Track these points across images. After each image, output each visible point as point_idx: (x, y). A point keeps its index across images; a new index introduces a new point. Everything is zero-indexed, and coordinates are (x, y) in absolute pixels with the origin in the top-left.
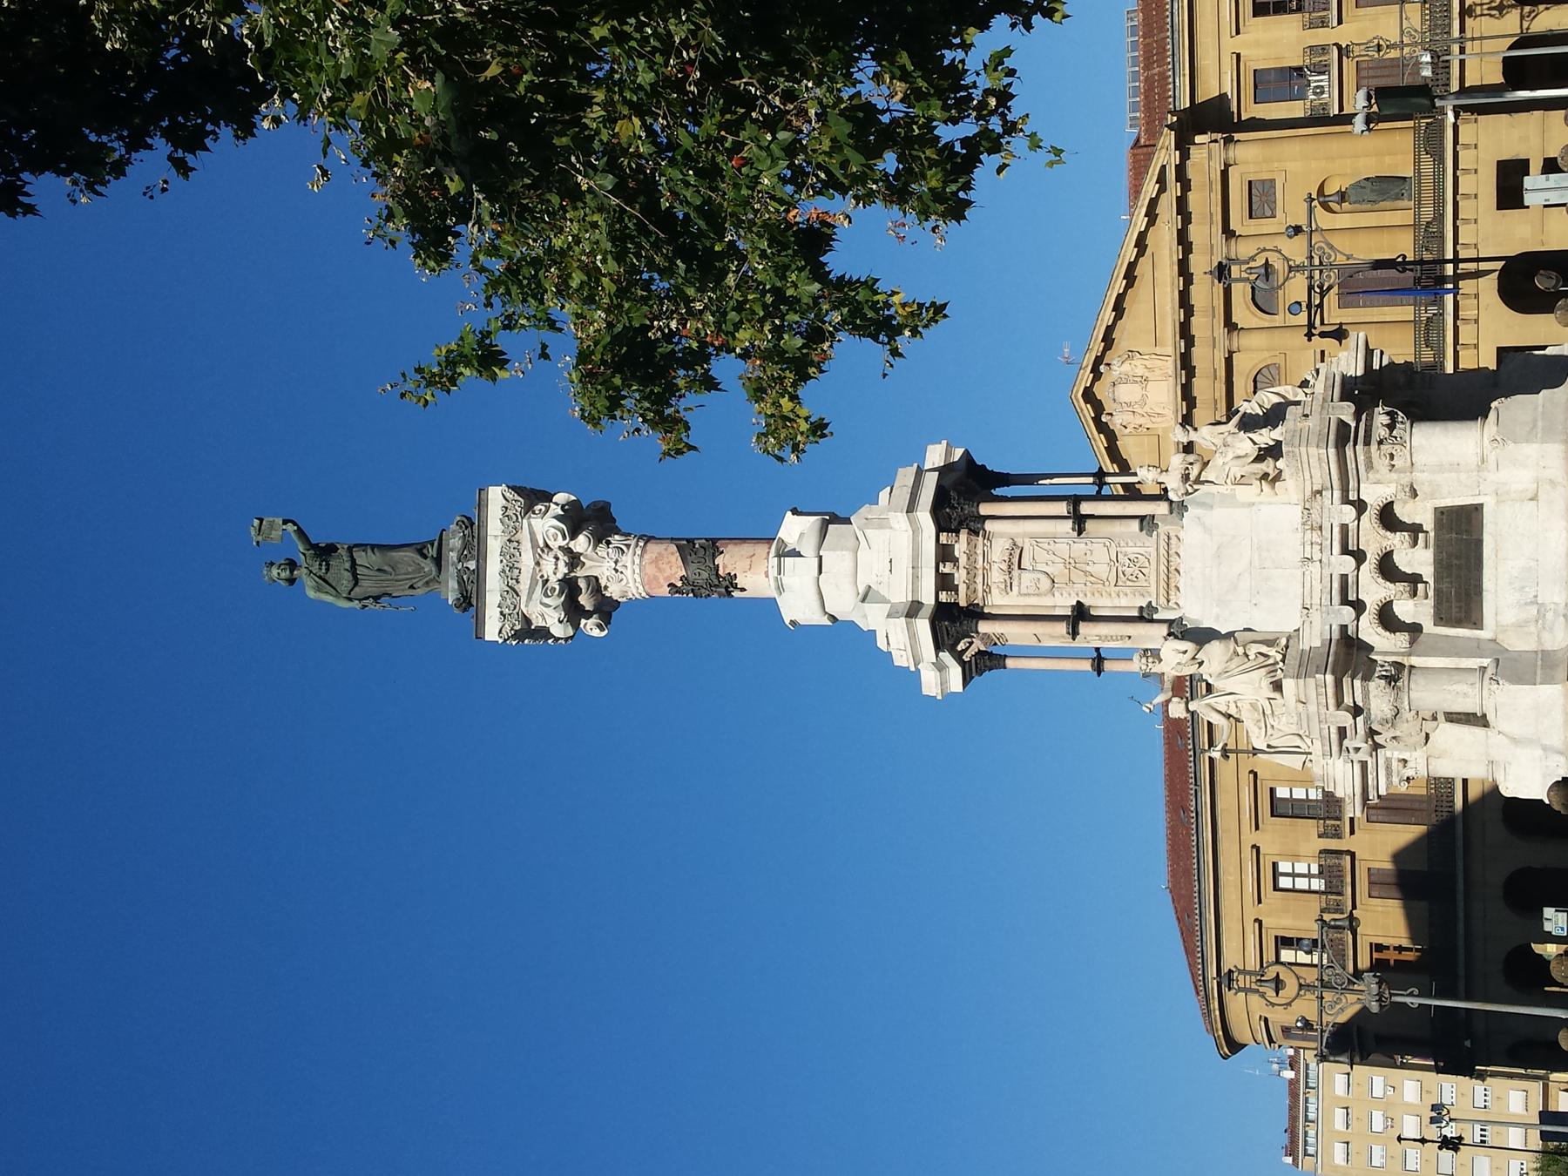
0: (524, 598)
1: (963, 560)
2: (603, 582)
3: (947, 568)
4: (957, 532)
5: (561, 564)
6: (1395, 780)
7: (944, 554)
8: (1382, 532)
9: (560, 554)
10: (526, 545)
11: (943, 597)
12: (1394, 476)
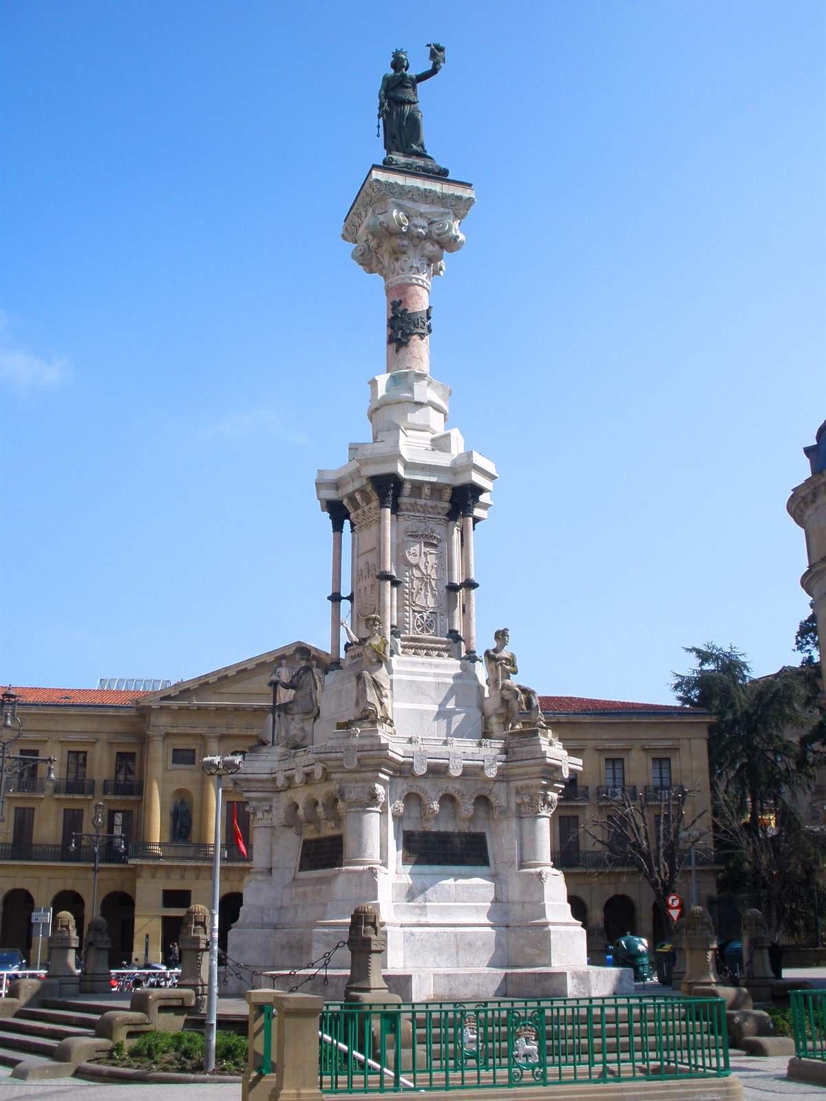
0: (397, 201)
1: (430, 503)
2: (404, 257)
3: (426, 491)
4: (450, 502)
5: (420, 230)
6: (254, 804)
7: (436, 489)
8: (475, 796)
9: (427, 230)
10: (435, 209)
11: (407, 486)
12: (513, 806)
